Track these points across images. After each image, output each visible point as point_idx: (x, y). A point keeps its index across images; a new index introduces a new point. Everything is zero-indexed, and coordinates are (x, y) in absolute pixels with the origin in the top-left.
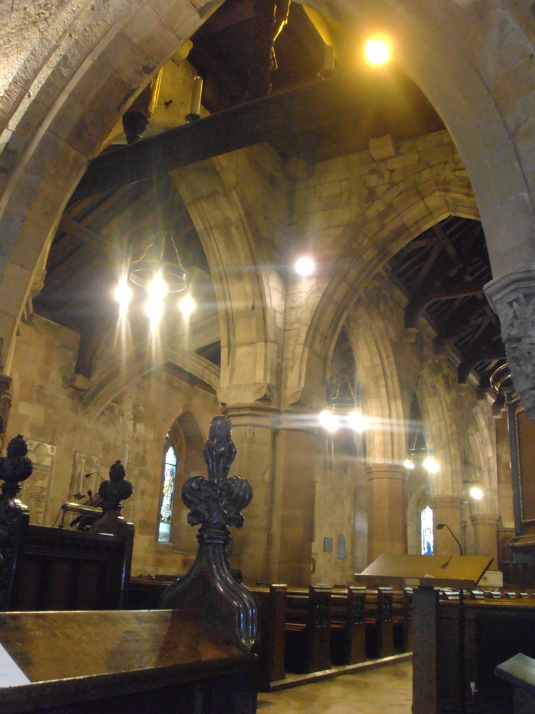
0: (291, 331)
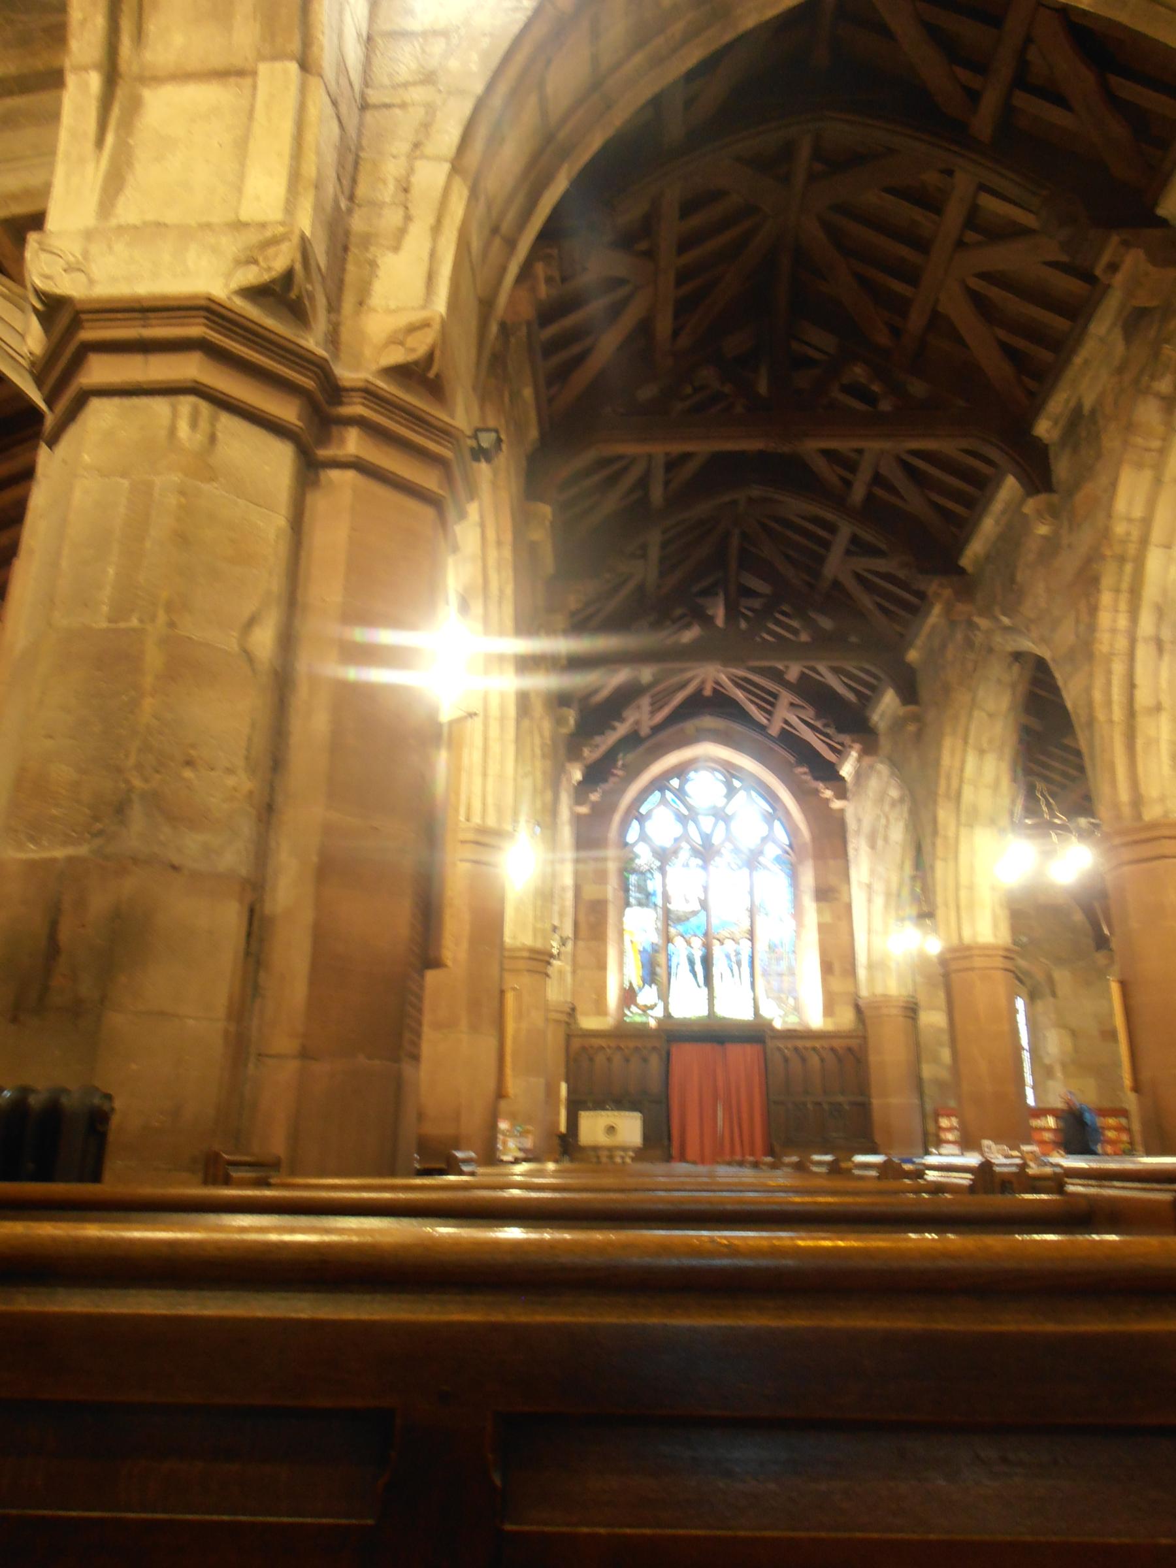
0: (397, 111)
